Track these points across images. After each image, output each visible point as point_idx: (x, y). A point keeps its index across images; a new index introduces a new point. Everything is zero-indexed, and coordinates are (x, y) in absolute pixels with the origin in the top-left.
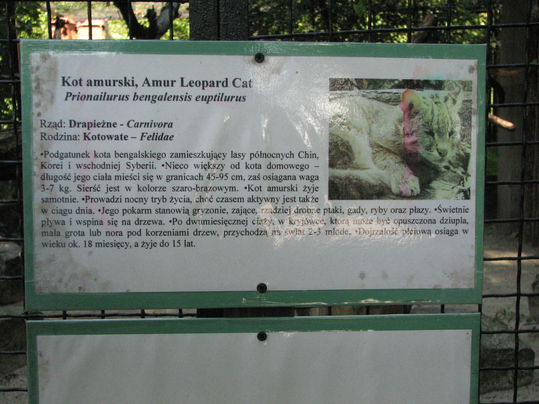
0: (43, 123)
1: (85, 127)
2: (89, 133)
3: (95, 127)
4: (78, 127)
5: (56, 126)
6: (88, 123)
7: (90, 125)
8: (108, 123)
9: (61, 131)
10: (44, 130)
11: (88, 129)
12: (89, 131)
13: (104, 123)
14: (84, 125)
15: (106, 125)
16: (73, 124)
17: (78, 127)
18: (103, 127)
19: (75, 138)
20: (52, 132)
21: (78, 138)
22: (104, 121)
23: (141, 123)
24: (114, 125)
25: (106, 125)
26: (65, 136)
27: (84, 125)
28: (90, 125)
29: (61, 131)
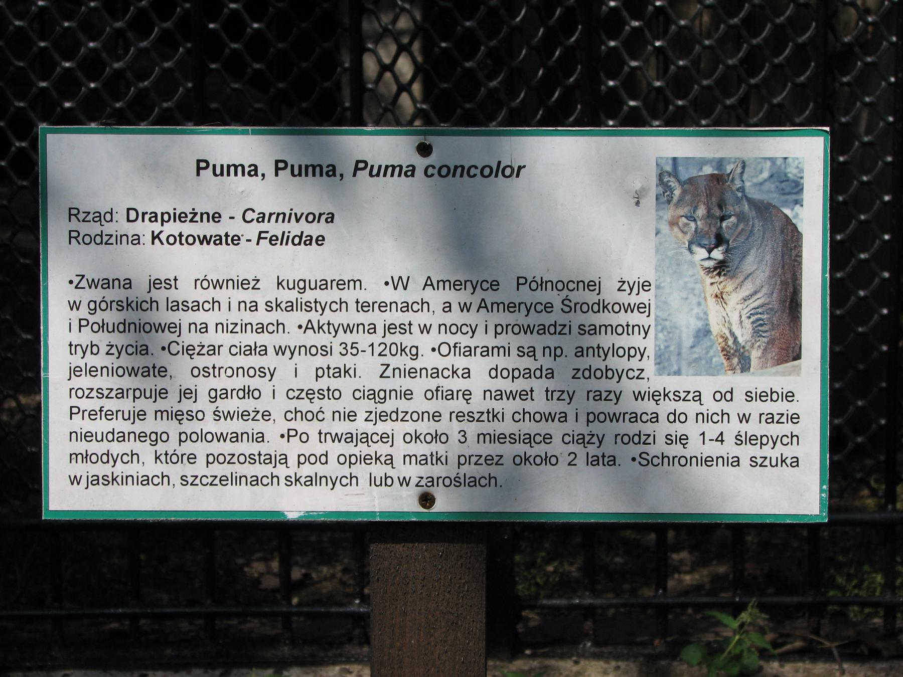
0: (73, 213)
1: (156, 221)
2: (161, 232)
3: (175, 221)
4: (143, 221)
5: (99, 217)
6: (163, 214)
7: (166, 217)
8: (202, 214)
10: (74, 225)
11: (162, 225)
12: (162, 228)
13: (196, 214)
14: (154, 217)
15: (198, 218)
16: (133, 215)
17: (143, 221)
18: (191, 221)
20: (94, 229)
22: (193, 209)
23: (271, 215)
24: (216, 217)
25: (198, 218)
26: (117, 236)
27: (154, 217)
28: (166, 217)
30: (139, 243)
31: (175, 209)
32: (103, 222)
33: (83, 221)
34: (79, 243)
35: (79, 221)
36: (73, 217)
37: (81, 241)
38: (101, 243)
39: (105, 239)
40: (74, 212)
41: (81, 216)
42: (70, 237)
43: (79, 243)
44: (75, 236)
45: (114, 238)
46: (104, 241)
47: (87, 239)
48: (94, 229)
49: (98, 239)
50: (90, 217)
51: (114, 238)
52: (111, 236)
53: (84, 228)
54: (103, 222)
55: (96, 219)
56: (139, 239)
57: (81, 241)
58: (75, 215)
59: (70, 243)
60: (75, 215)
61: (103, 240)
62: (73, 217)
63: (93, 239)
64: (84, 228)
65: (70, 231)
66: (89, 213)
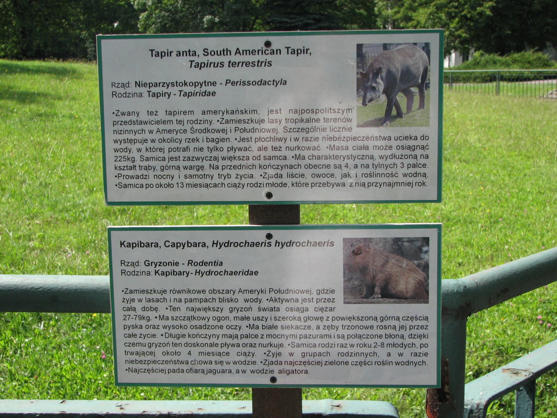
0: (122, 263)
5: (133, 264)
9: (137, 269)
10: (123, 267)
16: (148, 263)
19: (149, 274)
20: (131, 269)
29: (137, 269)
32: (135, 266)
36: (122, 264)
40: (123, 262)
41: (126, 264)
42: (122, 273)
44: (123, 272)
45: (140, 273)
48: (131, 269)
49: (133, 273)
52: (138, 272)
54: (135, 266)
58: (124, 263)
60: (124, 263)
63: (131, 273)
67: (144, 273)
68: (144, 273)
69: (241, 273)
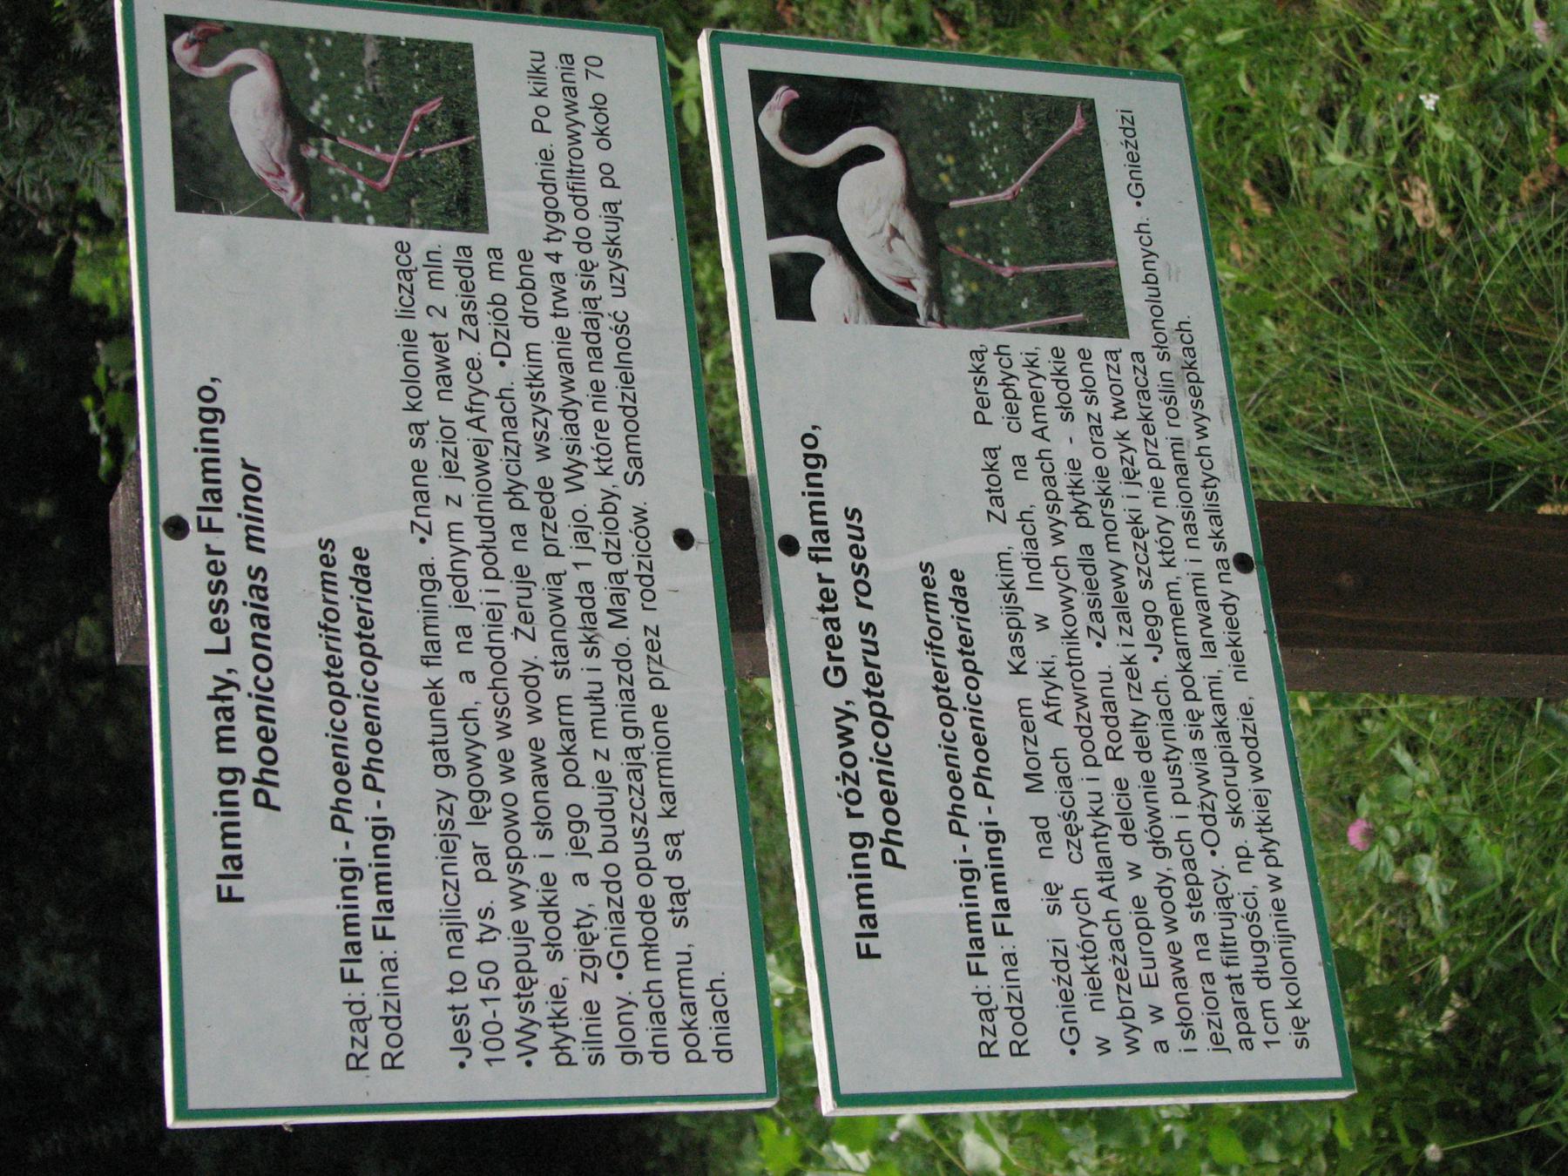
0: (355, 1064)
5: (359, 1022)
9: (375, 1007)
10: (374, 1061)
19: (390, 963)
20: (377, 1031)
21: (393, 956)
29: (375, 1007)
30: (394, 960)
31: (338, 907)
33: (366, 1046)
34: (401, 1053)
35: (366, 1054)
36: (362, 1064)
37: (399, 1050)
38: (399, 1018)
39: (391, 1012)
41: (359, 1051)
42: (393, 1067)
43: (401, 1053)
44: (391, 1063)
45: (389, 999)
46: (395, 1014)
47: (394, 1040)
48: (377, 1031)
49: (393, 1023)
50: (360, 1037)
51: (389, 999)
52: (386, 1003)
53: (378, 1046)
55: (362, 1026)
56: (388, 960)
57: (399, 1050)
59: (402, 1067)
61: (393, 1016)
62: (362, 1064)
64: (378, 1046)
65: (384, 1068)
66: (353, 1039)
67: (388, 982)
68: (389, 982)
69: (364, 605)
